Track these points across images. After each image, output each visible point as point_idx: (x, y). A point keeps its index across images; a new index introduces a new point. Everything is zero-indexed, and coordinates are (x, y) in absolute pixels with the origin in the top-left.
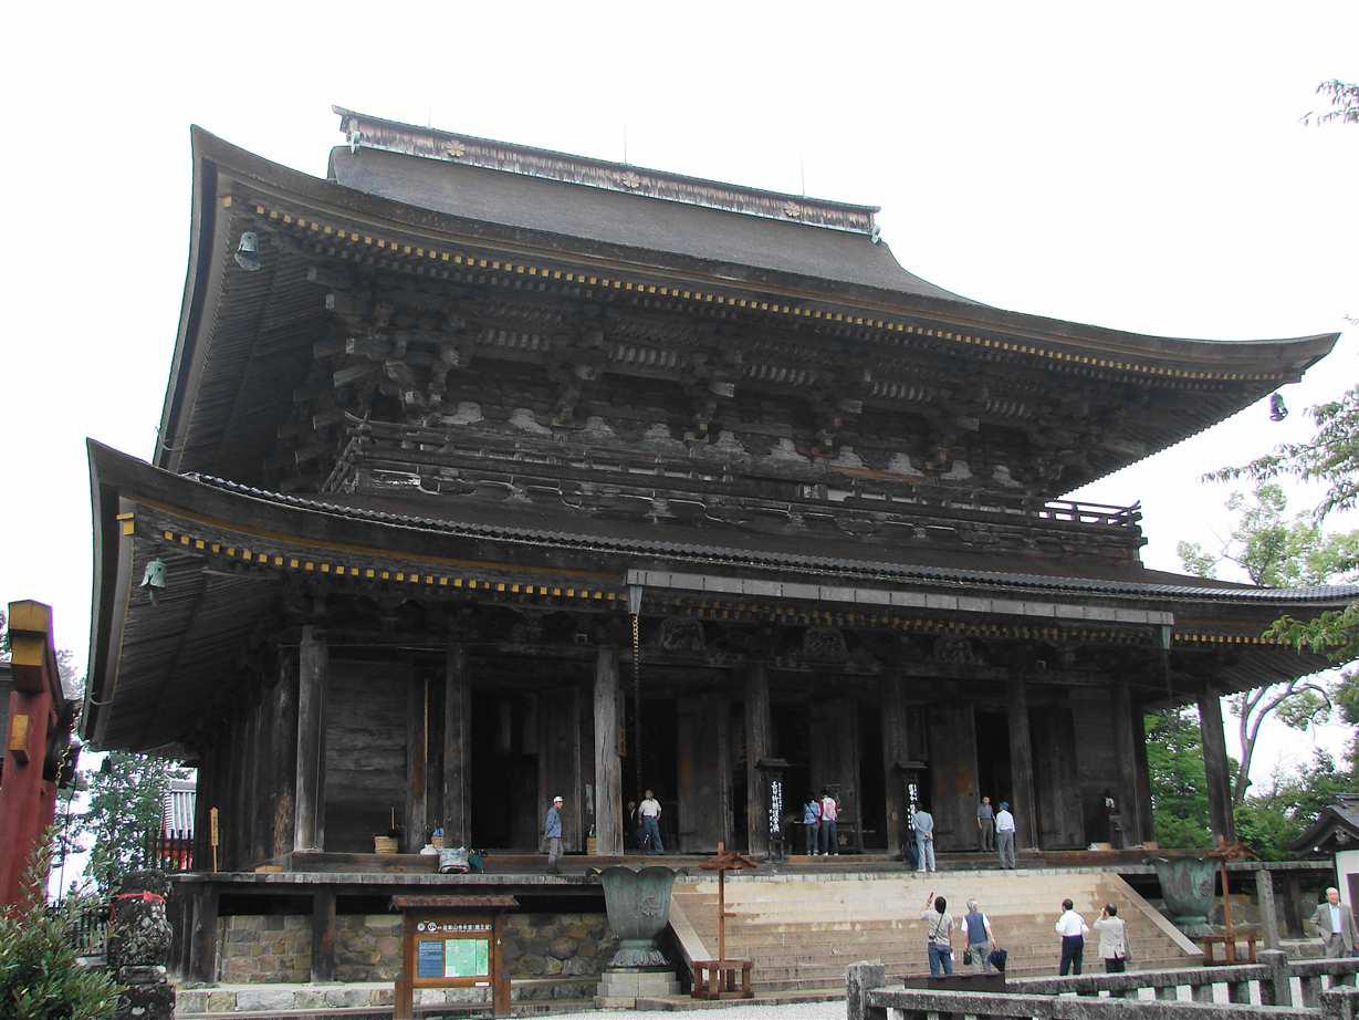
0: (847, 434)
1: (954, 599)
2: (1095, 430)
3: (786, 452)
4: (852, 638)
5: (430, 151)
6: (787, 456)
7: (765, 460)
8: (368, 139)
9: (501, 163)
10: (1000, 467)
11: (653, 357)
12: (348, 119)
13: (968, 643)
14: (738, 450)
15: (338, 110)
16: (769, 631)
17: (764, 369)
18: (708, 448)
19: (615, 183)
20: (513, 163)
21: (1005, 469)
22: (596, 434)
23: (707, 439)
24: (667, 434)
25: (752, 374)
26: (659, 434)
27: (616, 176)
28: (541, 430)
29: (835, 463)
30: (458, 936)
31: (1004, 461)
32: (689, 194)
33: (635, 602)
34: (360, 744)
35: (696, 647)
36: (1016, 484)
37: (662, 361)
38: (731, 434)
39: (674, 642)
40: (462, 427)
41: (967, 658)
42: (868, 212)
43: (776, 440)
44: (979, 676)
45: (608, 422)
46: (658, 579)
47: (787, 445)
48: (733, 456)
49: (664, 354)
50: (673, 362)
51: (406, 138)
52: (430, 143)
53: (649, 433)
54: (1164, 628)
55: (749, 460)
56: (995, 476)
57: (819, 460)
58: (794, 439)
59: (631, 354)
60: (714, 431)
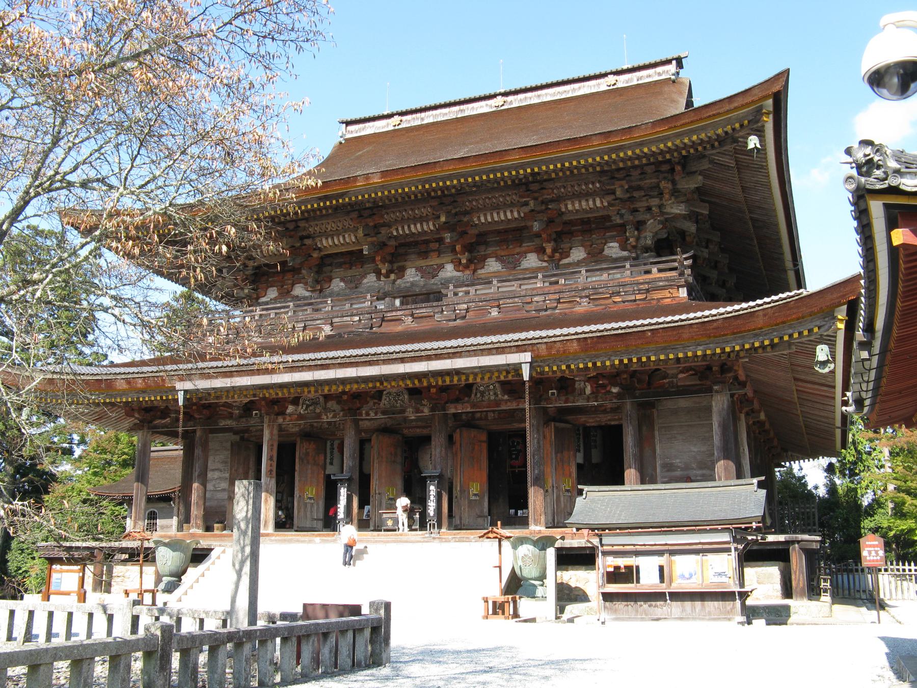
0: (490, 250)
1: (354, 369)
2: (655, 202)
3: (449, 271)
4: (414, 392)
6: (449, 275)
7: (433, 281)
10: (611, 244)
11: (341, 239)
13: (497, 385)
14: (417, 278)
16: (345, 397)
17: (406, 227)
18: (399, 281)
21: (616, 245)
22: (336, 289)
23: (393, 276)
24: (375, 279)
25: (401, 232)
26: (371, 279)
28: (307, 294)
29: (480, 272)
30: (67, 571)
31: (613, 239)
33: (181, 397)
34: (216, 477)
35: (318, 411)
36: (625, 253)
37: (348, 240)
38: (414, 270)
39: (306, 409)
40: (267, 303)
41: (495, 394)
43: (441, 267)
44: (503, 407)
45: (342, 280)
46: (188, 385)
47: (449, 267)
48: (413, 284)
49: (346, 236)
53: (365, 281)
54: (523, 365)
55: (422, 282)
56: (607, 252)
57: (468, 272)
58: (452, 262)
59: (330, 240)
60: (401, 271)
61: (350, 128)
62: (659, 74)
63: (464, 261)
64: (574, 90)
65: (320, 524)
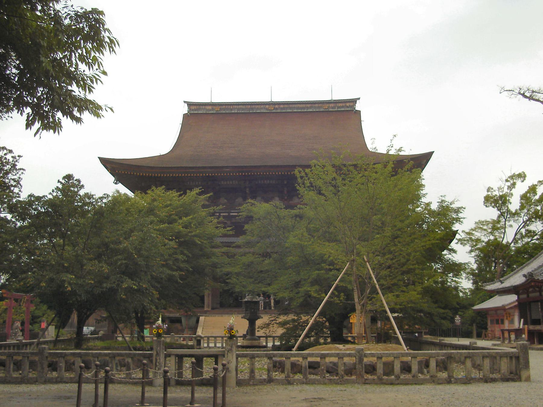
5: (210, 110)
8: (193, 110)
9: (231, 110)
12: (190, 104)
15: (185, 102)
19: (267, 109)
20: (235, 109)
27: (267, 106)
29: (290, 202)
32: (290, 108)
42: (354, 101)
45: (226, 199)
50: (237, 182)
51: (203, 107)
52: (210, 107)
53: (237, 200)
61: (193, 108)
62: (348, 107)
63: (286, 198)
64: (308, 108)
65: (218, 306)
